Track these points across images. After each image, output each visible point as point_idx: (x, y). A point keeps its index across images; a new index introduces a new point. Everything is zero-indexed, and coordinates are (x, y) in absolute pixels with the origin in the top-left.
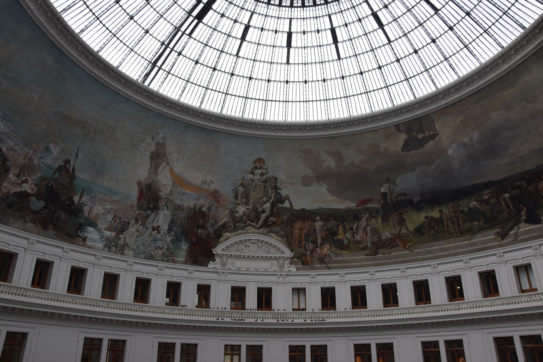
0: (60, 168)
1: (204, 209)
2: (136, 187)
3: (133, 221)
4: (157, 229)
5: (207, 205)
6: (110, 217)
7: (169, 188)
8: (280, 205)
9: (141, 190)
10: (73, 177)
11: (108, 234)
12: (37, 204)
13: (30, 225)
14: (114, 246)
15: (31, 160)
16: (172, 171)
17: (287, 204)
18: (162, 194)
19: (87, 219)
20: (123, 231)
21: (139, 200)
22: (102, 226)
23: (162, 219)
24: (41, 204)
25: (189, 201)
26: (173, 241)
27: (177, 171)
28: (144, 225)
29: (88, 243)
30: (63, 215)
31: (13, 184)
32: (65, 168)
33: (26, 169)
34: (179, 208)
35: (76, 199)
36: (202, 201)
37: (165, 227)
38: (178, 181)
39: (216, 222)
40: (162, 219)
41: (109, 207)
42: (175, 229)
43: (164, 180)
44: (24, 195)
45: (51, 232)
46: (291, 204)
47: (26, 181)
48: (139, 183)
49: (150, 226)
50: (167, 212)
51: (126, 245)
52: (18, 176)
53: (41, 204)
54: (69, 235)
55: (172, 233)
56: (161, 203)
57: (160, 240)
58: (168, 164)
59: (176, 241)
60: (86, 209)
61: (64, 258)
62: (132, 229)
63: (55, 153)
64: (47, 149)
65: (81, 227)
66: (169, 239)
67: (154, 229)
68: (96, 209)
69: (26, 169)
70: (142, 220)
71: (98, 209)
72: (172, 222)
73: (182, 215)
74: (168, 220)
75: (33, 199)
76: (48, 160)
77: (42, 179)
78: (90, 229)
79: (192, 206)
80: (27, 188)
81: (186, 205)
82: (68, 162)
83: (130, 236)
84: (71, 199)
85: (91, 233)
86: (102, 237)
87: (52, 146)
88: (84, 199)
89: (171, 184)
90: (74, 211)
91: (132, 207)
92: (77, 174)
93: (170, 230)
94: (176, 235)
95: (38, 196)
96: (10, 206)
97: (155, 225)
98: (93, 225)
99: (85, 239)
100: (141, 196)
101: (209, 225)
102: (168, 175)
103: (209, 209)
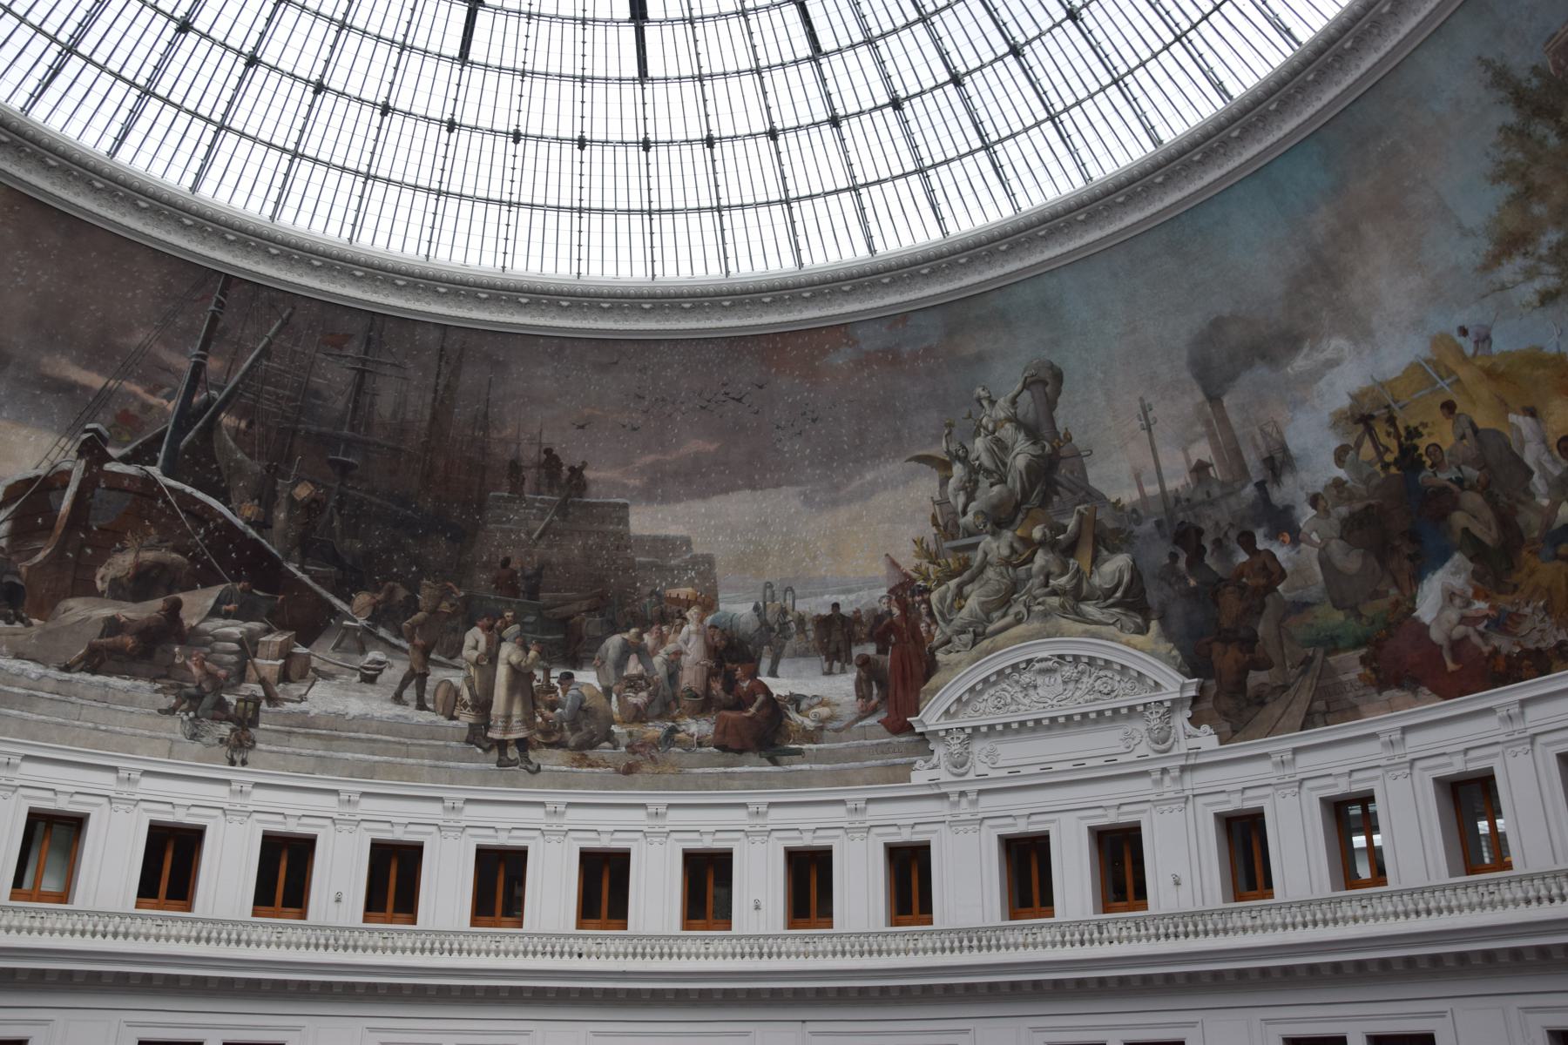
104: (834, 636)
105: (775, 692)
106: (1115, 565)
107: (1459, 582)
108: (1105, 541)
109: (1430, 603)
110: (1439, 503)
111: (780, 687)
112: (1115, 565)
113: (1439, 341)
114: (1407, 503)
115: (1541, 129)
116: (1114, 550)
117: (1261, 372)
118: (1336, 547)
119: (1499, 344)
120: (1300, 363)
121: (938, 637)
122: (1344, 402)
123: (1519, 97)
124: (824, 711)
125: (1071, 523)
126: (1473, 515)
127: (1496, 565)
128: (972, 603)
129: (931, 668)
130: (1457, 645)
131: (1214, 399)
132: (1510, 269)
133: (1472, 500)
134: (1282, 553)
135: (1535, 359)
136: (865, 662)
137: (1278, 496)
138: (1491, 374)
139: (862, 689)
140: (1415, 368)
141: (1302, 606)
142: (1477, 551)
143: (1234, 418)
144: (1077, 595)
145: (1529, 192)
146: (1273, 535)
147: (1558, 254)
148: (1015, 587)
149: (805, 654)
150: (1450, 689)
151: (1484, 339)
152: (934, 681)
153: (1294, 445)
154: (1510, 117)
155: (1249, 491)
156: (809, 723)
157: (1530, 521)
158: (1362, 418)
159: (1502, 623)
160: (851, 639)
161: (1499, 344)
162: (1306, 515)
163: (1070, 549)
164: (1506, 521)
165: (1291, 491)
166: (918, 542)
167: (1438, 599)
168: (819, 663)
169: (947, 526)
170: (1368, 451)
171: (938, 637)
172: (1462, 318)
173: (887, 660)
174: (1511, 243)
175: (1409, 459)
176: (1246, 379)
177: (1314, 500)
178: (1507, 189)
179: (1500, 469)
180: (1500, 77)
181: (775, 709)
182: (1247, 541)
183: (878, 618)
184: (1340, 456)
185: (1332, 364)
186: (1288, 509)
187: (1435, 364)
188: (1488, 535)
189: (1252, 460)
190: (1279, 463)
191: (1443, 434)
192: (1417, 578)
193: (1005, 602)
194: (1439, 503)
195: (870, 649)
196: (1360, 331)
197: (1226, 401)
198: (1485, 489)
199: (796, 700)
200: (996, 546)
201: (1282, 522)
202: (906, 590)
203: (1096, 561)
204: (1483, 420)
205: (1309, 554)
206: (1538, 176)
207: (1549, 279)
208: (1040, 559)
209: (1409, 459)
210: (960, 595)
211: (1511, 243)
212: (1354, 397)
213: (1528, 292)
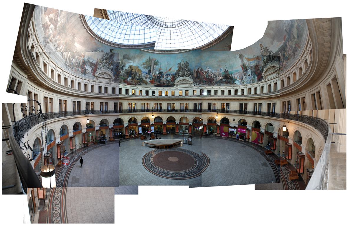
0: (225, 72)
1: (257, 64)
2: (241, 67)
3: (244, 76)
4: (249, 75)
5: (257, 62)
6: (239, 77)
7: (247, 63)
8: (271, 54)
9: (242, 67)
10: (228, 72)
11: (240, 81)
12: (224, 80)
13: (225, 84)
14: (242, 83)
15: (219, 73)
16: (246, 58)
17: (272, 53)
18: (247, 66)
19: (235, 79)
20: (242, 79)
21: (243, 70)
22: (238, 79)
23: (249, 72)
24: (225, 80)
25: (253, 64)
26: (254, 77)
27: (247, 57)
28: (246, 76)
29: (237, 84)
30: (230, 80)
31: (219, 78)
32: (226, 71)
33: (219, 75)
34: (251, 67)
35: (231, 76)
36: (256, 62)
37: (251, 74)
38: (248, 60)
39: (261, 66)
40: (249, 72)
41: (238, 75)
42: (253, 73)
43: (245, 61)
44: (221, 80)
45: (229, 84)
46: (273, 52)
47: (220, 77)
48: (241, 66)
49: (247, 75)
50: (250, 70)
51: (244, 82)
52: (219, 76)
53: (225, 80)
54: (233, 84)
55: (253, 75)
56: (248, 68)
57: (251, 78)
58: (244, 57)
59: (254, 76)
60: (234, 77)
61: (233, 89)
62: (244, 78)
63: (222, 69)
64: (220, 69)
65: (234, 81)
66: (252, 77)
67: (249, 75)
68: (235, 76)
69: (219, 75)
70: (245, 74)
71: (236, 76)
72: (252, 72)
73: (253, 69)
74: (251, 72)
75: (223, 79)
76: (222, 71)
77: (223, 75)
78: (236, 81)
79: (254, 65)
80: (221, 78)
81: (253, 65)
82: (225, 69)
83: (244, 80)
84: (230, 76)
85: (236, 82)
86: (239, 82)
87: (221, 68)
88: (232, 75)
89: (247, 61)
90: (232, 78)
91: (242, 72)
92: (229, 71)
93: (252, 74)
94: (254, 75)
95: (224, 78)
96: (220, 82)
97: (248, 74)
98: (236, 80)
99: (236, 84)
100: (243, 69)
101: (260, 68)
102: (245, 59)
103: (258, 63)
104: (92, 64)
105: (86, 68)
106: (112, 67)
107: (131, 79)
108: (112, 64)
109: (128, 79)
110: (132, 74)
111: (86, 68)
112: (112, 67)
113: (137, 66)
114: (130, 73)
115: (149, 61)
116: (112, 65)
117: (127, 60)
118: (125, 73)
119: (140, 68)
120: (129, 61)
121: (98, 68)
122: (130, 65)
123: (149, 59)
124: (89, 72)
125: (111, 62)
126: (133, 76)
127: (133, 79)
128: (101, 66)
129: (97, 70)
130: (129, 82)
131: (123, 59)
132: (143, 65)
133: (133, 75)
134: (122, 71)
135: (140, 70)
136: (93, 68)
137: (123, 68)
138: (138, 69)
139: (92, 70)
140: (135, 66)
141: (121, 75)
142: (132, 77)
143: (124, 61)
144: (108, 68)
145: (146, 63)
146: (122, 70)
147: (145, 66)
148: (104, 66)
149: (89, 65)
150: (128, 84)
151: (139, 67)
152: (97, 72)
153: (126, 65)
154: (148, 59)
155: (122, 66)
156: (87, 72)
157: (136, 77)
158: (130, 67)
159: (132, 82)
160: (92, 65)
161: (140, 68)
162: (124, 70)
163: (109, 64)
164: (134, 77)
165: (124, 68)
166: (100, 58)
167: (129, 79)
168: (89, 67)
169: (102, 58)
170: (130, 69)
171: (98, 68)
172: (139, 66)
173: (94, 68)
174: (144, 64)
175: (131, 71)
176: (126, 59)
177: (125, 69)
178: (145, 62)
179: (136, 74)
180: (150, 57)
181: (86, 70)
182: (120, 69)
183: (95, 64)
184: (128, 68)
185: (131, 63)
186: (123, 69)
187: (136, 67)
188: (133, 77)
189: (123, 64)
190: (124, 66)
191: (134, 70)
192: (128, 77)
193: (103, 67)
194: (132, 74)
195: (93, 67)
196: (134, 62)
197: (124, 60)
198: (134, 75)
199: (87, 70)
200: (105, 61)
201: (123, 70)
202: (97, 63)
203: (111, 66)
204: (136, 71)
205: (123, 73)
206: (147, 63)
207: (144, 67)
208: (107, 64)
209: (131, 71)
210: (101, 65)
211: (144, 64)
212: (131, 65)
213: (143, 67)
